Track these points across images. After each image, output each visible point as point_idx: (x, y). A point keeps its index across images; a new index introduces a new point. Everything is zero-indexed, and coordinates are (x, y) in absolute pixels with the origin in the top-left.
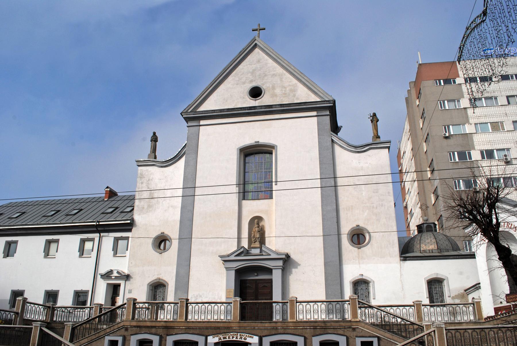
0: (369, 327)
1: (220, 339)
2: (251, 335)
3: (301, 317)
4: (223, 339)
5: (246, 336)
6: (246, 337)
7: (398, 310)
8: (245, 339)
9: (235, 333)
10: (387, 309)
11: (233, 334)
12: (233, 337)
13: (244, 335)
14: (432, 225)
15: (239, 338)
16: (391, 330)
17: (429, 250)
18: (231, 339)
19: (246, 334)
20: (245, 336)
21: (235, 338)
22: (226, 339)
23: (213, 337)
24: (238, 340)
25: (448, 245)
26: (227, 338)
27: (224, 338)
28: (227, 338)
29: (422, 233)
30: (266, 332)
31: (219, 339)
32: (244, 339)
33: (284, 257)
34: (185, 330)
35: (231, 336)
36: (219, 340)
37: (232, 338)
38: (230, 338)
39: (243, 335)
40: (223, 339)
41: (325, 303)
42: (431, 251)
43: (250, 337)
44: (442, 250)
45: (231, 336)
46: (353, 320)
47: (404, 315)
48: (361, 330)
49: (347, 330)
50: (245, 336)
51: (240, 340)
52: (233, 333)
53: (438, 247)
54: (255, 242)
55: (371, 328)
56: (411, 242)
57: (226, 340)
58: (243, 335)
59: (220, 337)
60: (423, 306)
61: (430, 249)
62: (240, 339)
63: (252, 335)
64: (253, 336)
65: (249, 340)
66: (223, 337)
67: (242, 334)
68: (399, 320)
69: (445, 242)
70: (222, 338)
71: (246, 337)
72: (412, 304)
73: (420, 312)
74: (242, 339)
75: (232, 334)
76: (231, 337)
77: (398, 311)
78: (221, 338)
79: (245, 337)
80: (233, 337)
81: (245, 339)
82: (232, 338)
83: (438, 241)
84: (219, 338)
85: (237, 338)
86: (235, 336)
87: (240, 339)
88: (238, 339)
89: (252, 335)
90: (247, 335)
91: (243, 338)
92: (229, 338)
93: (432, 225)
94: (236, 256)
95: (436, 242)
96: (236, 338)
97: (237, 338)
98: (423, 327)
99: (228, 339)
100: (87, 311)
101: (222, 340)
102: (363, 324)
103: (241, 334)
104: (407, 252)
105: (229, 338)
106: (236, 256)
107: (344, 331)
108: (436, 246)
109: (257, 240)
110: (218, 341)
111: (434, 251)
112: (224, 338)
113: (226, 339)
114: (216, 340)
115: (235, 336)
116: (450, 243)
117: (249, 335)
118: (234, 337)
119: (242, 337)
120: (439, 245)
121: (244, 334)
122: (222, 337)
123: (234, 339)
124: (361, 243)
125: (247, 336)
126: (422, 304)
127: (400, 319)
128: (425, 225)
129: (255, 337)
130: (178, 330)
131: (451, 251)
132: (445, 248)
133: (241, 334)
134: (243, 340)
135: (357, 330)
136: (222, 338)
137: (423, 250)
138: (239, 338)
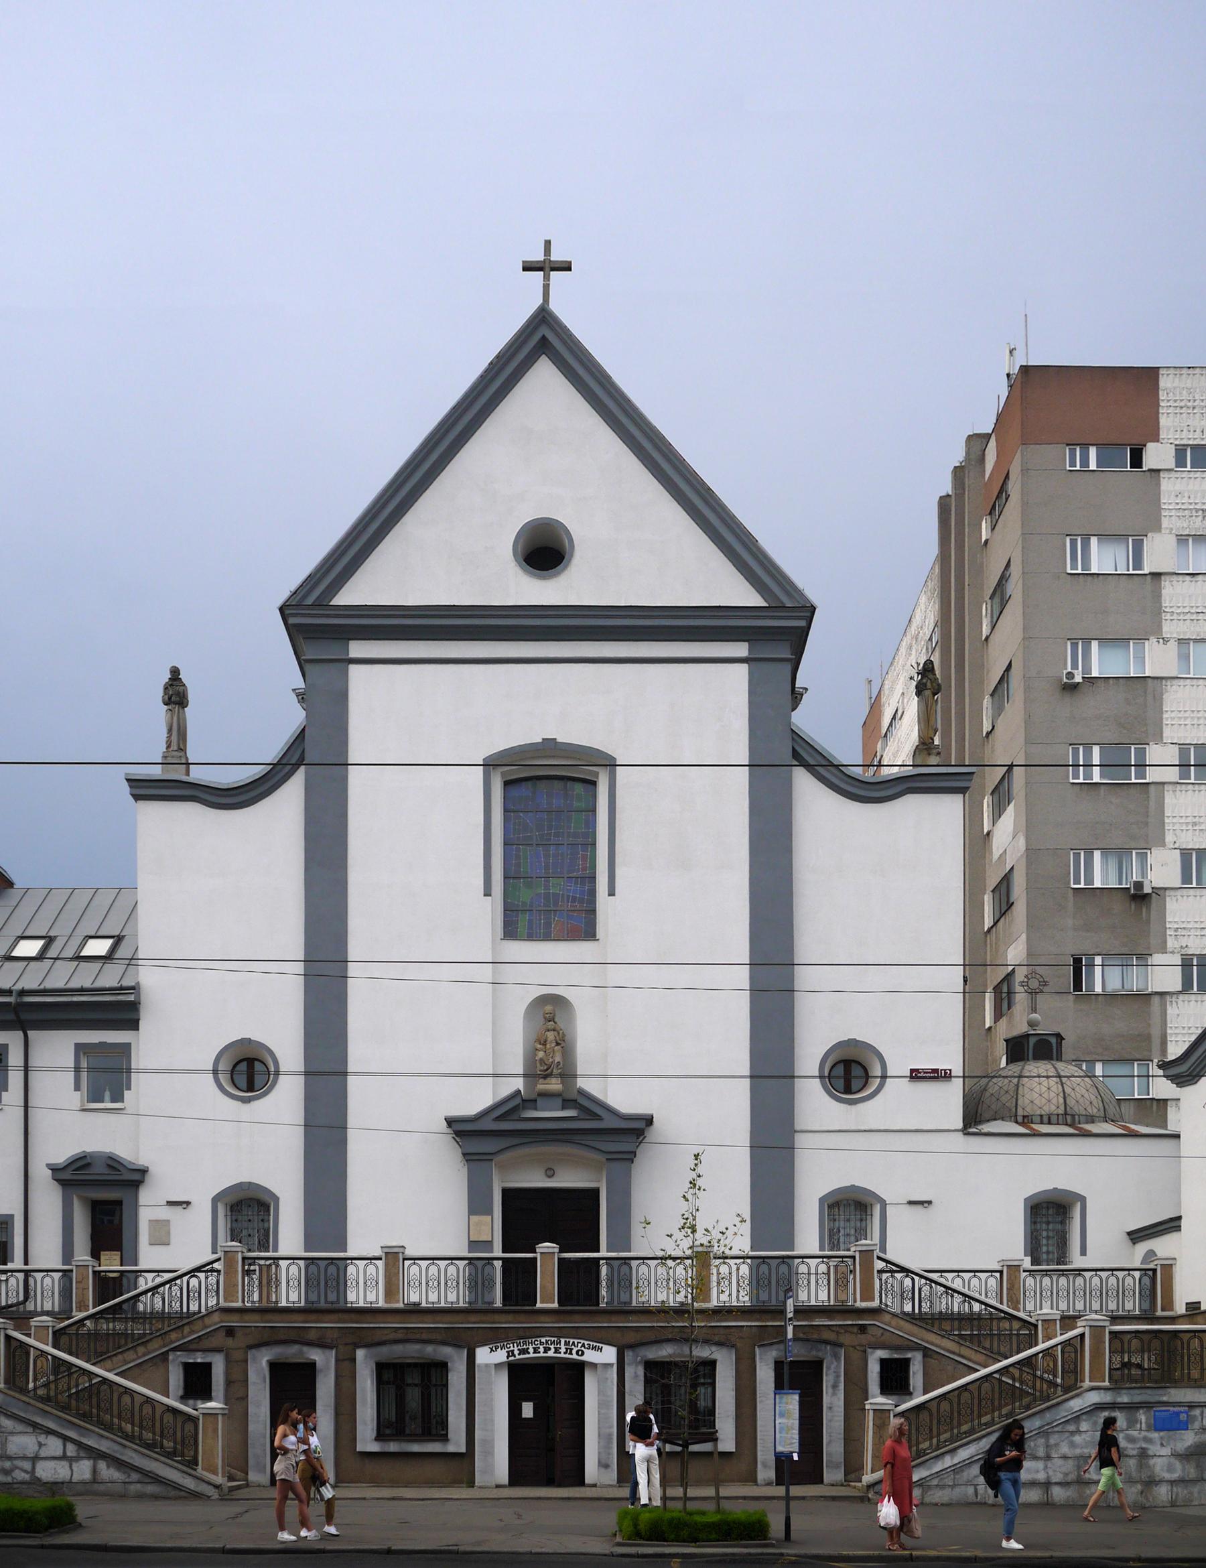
0: (902, 1323)
1: (511, 1353)
2: (595, 1344)
3: (724, 1297)
4: (519, 1354)
5: (583, 1345)
6: (583, 1349)
7: (975, 1282)
8: (580, 1353)
9: (553, 1339)
10: (947, 1279)
11: (547, 1342)
12: (546, 1350)
13: (578, 1343)
14: (1053, 1040)
15: (563, 1350)
16: (956, 1333)
17: (1041, 1116)
18: (542, 1354)
19: (582, 1342)
20: (580, 1345)
21: (553, 1350)
22: (529, 1353)
23: (492, 1350)
24: (562, 1355)
25: (1095, 1102)
26: (531, 1350)
27: (522, 1352)
28: (531, 1350)
29: (1021, 1063)
30: (631, 1338)
31: (509, 1354)
32: (577, 1353)
33: (641, 1125)
34: (405, 1331)
35: (541, 1347)
36: (508, 1357)
37: (545, 1352)
38: (539, 1352)
39: (574, 1342)
40: (519, 1354)
41: (749, 1261)
42: (1045, 1119)
43: (594, 1348)
44: (1077, 1117)
45: (541, 1347)
46: (864, 1305)
47: (989, 1294)
48: (882, 1331)
49: (846, 1331)
50: (580, 1345)
51: (567, 1356)
52: (548, 1339)
53: (1068, 1109)
54: (545, 1077)
55: (908, 1326)
56: (990, 1091)
57: (527, 1356)
58: (574, 1342)
59: (512, 1348)
60: (1024, 1271)
61: (1043, 1113)
62: (565, 1353)
63: (598, 1344)
64: (601, 1345)
65: (590, 1356)
66: (519, 1350)
67: (571, 1341)
68: (976, 1307)
69: (1086, 1095)
70: (516, 1352)
71: (583, 1349)
72: (998, 1267)
73: (1016, 1286)
74: (571, 1353)
75: (543, 1340)
76: (542, 1350)
77: (973, 1286)
78: (513, 1351)
79: (579, 1348)
80: (546, 1350)
81: (580, 1353)
82: (545, 1352)
83: (1068, 1090)
84: (508, 1352)
85: (557, 1351)
86: (552, 1347)
87: (565, 1353)
88: (560, 1353)
89: (595, 1342)
90: (586, 1343)
91: (574, 1352)
92: (536, 1351)
93: (1053, 1040)
94: (498, 1119)
95: (1062, 1095)
96: (555, 1352)
97: (557, 1351)
98: (1036, 1326)
99: (532, 1355)
100: (12, 1281)
101: (518, 1357)
102: (887, 1317)
103: (567, 1340)
104: (978, 1122)
105: (536, 1351)
106: (498, 1119)
107: (838, 1333)
108: (1062, 1108)
109: (554, 1071)
110: (505, 1359)
111: (1054, 1119)
112: (522, 1352)
113: (529, 1353)
114: (501, 1356)
115: (552, 1347)
116: (1099, 1097)
117: (591, 1343)
118: (550, 1349)
119: (571, 1350)
120: (1071, 1102)
121: (576, 1341)
122: (516, 1349)
123: (551, 1353)
124: (854, 1088)
125: (586, 1346)
126: (1024, 1266)
127: (977, 1304)
128: (1032, 1041)
129: (605, 1347)
130: (386, 1332)
131: (1100, 1122)
132: (1084, 1113)
133: (569, 1342)
134: (574, 1356)
135: (871, 1331)
136: (516, 1352)
137: (1024, 1117)
138: (563, 1350)
